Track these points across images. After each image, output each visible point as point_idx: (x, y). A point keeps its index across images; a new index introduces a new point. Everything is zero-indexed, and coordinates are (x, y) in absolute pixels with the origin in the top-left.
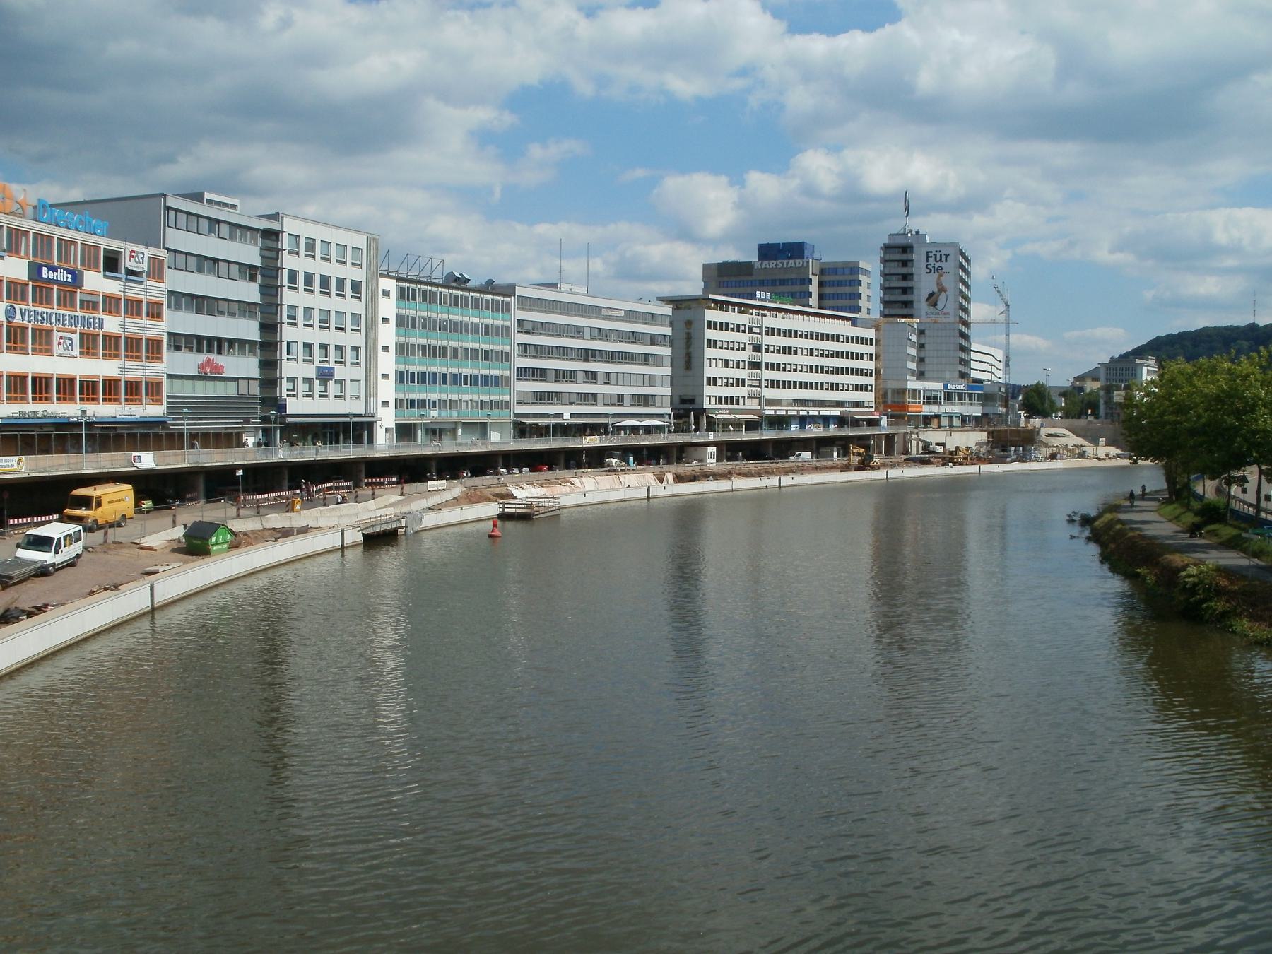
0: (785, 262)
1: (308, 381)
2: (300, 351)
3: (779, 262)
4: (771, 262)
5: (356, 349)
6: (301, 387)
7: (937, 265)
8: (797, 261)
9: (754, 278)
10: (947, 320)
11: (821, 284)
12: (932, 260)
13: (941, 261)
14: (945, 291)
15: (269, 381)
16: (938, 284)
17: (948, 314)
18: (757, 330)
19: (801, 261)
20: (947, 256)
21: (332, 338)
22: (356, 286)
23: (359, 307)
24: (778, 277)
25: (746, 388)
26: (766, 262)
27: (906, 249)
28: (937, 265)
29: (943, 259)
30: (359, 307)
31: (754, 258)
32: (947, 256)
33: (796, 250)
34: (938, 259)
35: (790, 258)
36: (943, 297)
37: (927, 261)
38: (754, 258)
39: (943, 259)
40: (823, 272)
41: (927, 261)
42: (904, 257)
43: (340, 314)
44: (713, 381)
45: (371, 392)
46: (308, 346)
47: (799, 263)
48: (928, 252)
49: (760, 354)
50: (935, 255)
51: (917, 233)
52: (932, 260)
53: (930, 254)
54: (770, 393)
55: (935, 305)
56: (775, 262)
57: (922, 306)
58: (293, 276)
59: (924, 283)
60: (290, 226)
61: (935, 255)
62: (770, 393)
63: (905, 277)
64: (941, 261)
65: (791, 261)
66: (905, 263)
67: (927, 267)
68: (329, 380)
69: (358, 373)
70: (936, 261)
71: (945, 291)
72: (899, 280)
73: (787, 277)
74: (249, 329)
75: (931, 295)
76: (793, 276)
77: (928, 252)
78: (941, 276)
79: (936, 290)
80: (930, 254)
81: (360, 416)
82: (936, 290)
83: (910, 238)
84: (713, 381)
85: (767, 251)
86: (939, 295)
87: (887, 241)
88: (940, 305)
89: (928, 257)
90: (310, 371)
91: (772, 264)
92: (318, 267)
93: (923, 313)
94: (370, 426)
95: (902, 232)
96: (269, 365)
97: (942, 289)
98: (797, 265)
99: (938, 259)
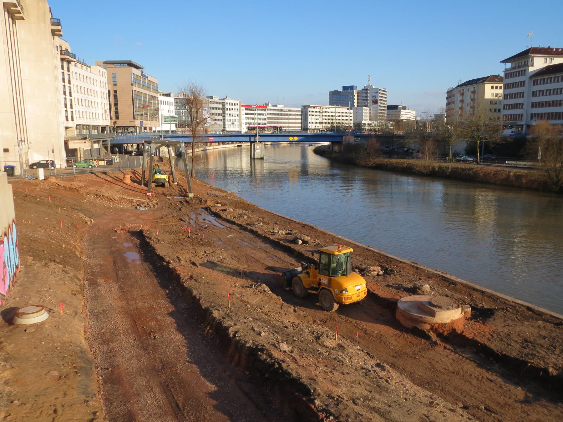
2: (229, 120)
6: (229, 126)
11: (358, 96)
15: (224, 125)
21: (234, 118)
22: (237, 109)
23: (238, 113)
27: (367, 90)
30: (238, 113)
40: (358, 93)
43: (235, 114)
45: (241, 126)
46: (230, 120)
58: (227, 109)
60: (227, 101)
69: (239, 123)
74: (221, 117)
85: (345, 88)
87: (363, 88)
90: (231, 123)
91: (345, 91)
92: (231, 107)
96: (224, 122)
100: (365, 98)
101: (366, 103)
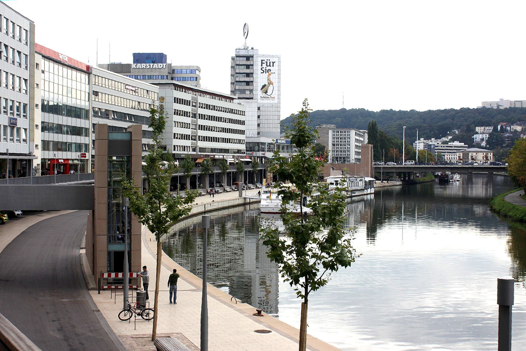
0: (152, 64)
1: (5, 127)
3: (148, 65)
4: (143, 64)
5: (25, 105)
7: (268, 68)
8: (159, 64)
9: (131, 74)
10: (274, 102)
12: (264, 65)
13: (270, 66)
14: (272, 84)
16: (268, 79)
17: (274, 98)
18: (194, 104)
19: (161, 64)
20: (273, 63)
24: (146, 74)
25: (191, 141)
26: (139, 64)
27: (248, 58)
28: (268, 68)
29: (271, 64)
31: (129, 60)
32: (273, 63)
33: (160, 58)
34: (268, 65)
35: (154, 62)
36: (270, 88)
37: (262, 66)
38: (129, 60)
39: (271, 64)
41: (262, 66)
42: (248, 63)
44: (175, 136)
47: (160, 65)
48: (262, 60)
49: (196, 119)
50: (267, 62)
51: (252, 49)
52: (264, 65)
53: (263, 62)
54: (201, 144)
55: (266, 92)
56: (145, 64)
57: (258, 93)
59: (260, 79)
61: (267, 62)
62: (201, 144)
63: (248, 75)
64: (270, 66)
65: (155, 64)
66: (248, 67)
67: (261, 69)
68: (14, 127)
70: (267, 65)
71: (272, 84)
72: (244, 76)
73: (152, 74)
75: (264, 86)
76: (157, 74)
77: (262, 60)
78: (270, 75)
79: (267, 83)
80: (263, 62)
81: (25, 155)
82: (267, 83)
83: (250, 53)
84: (175, 136)
85: (139, 58)
86: (268, 87)
88: (269, 92)
89: (262, 63)
91: (143, 65)
93: (259, 97)
94: (30, 161)
95: (243, 48)
97: (270, 83)
98: (159, 67)
99: (268, 65)
100: (247, 79)
101: (248, 92)
